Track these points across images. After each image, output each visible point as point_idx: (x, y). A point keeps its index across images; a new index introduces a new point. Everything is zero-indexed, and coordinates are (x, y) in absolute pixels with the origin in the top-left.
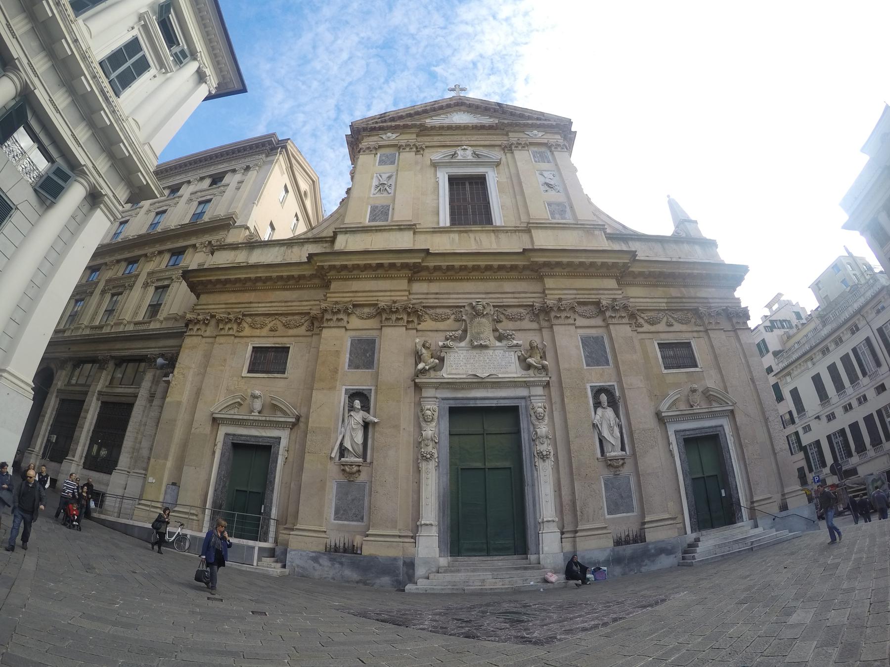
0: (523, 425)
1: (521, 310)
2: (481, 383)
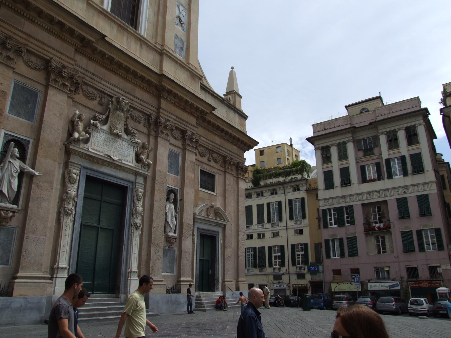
0: (128, 202)
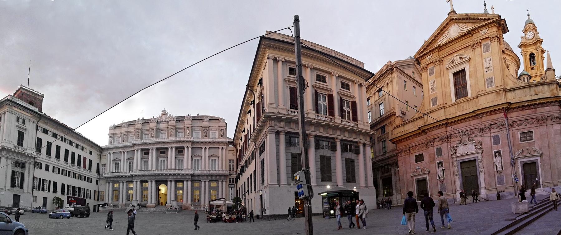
0: (477, 164)
1: (477, 130)
2: (466, 155)
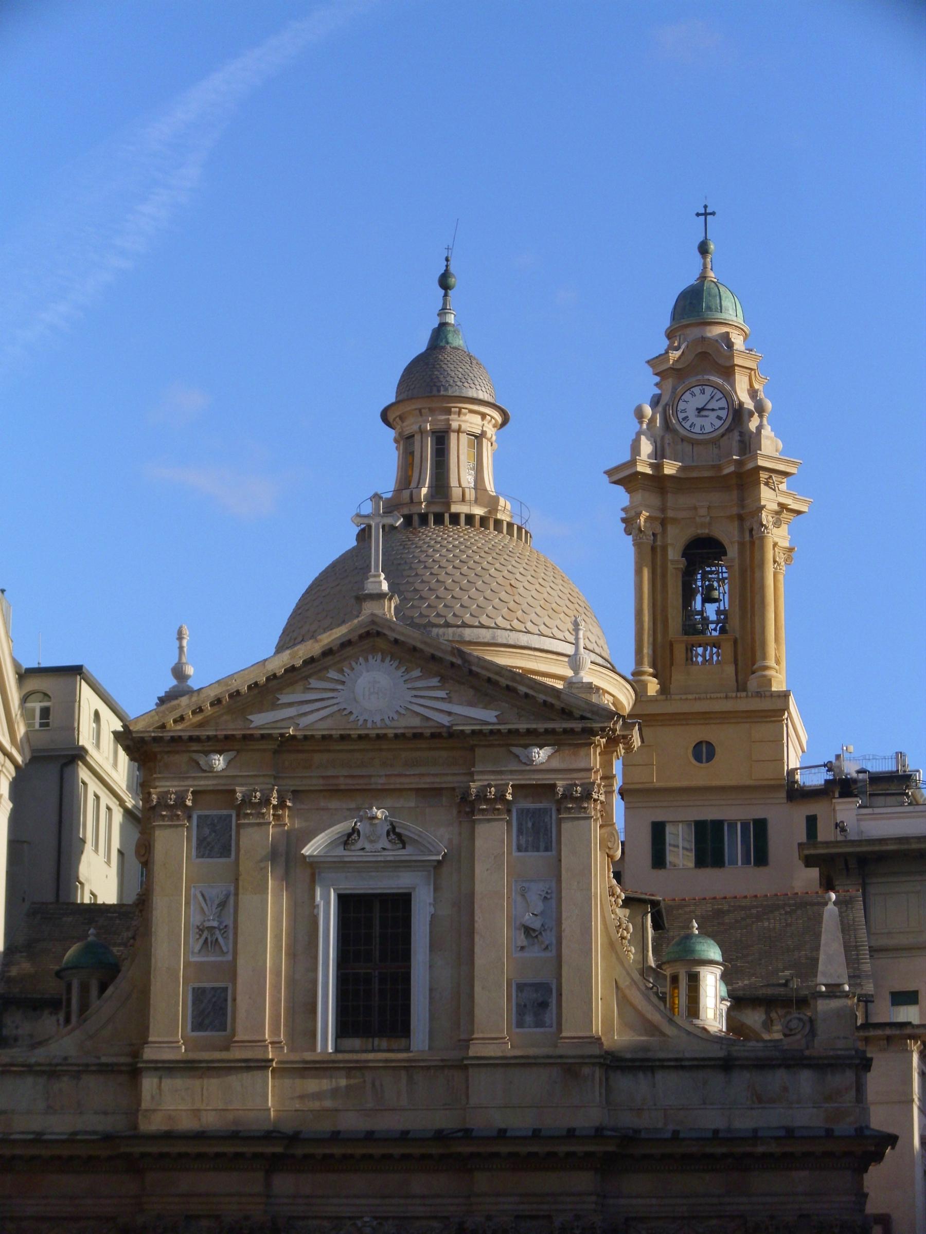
1: (435, 1224)
